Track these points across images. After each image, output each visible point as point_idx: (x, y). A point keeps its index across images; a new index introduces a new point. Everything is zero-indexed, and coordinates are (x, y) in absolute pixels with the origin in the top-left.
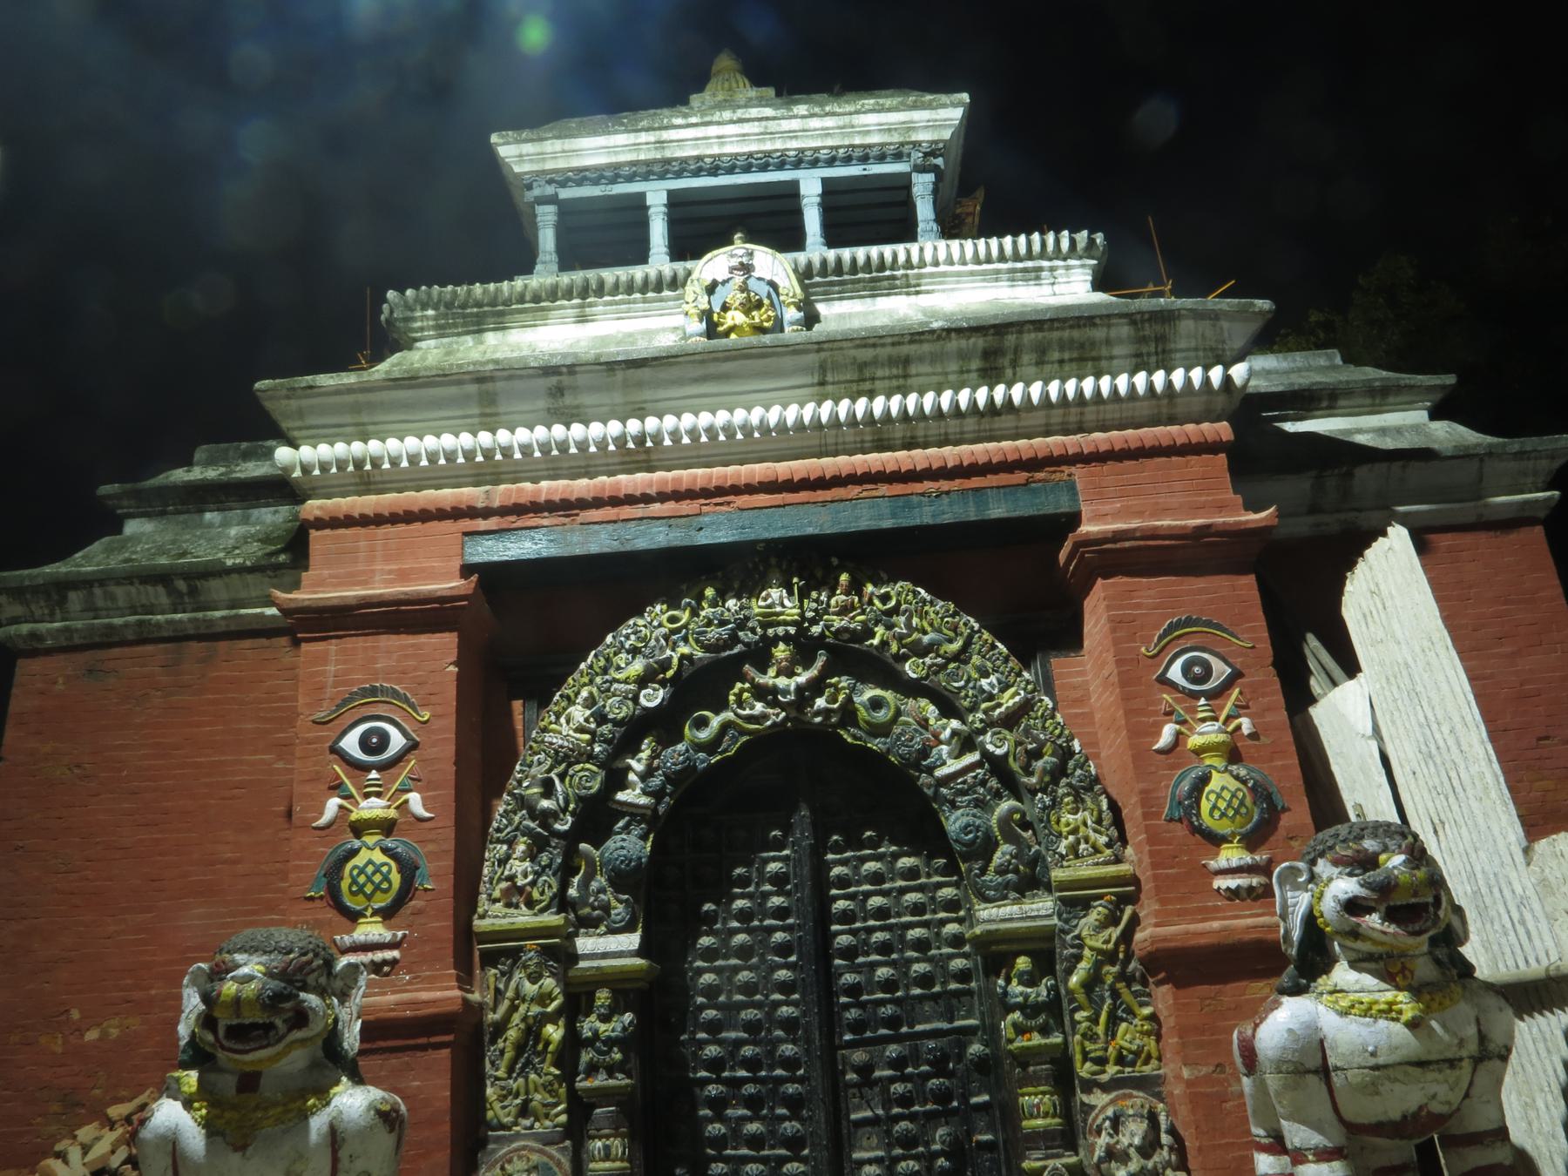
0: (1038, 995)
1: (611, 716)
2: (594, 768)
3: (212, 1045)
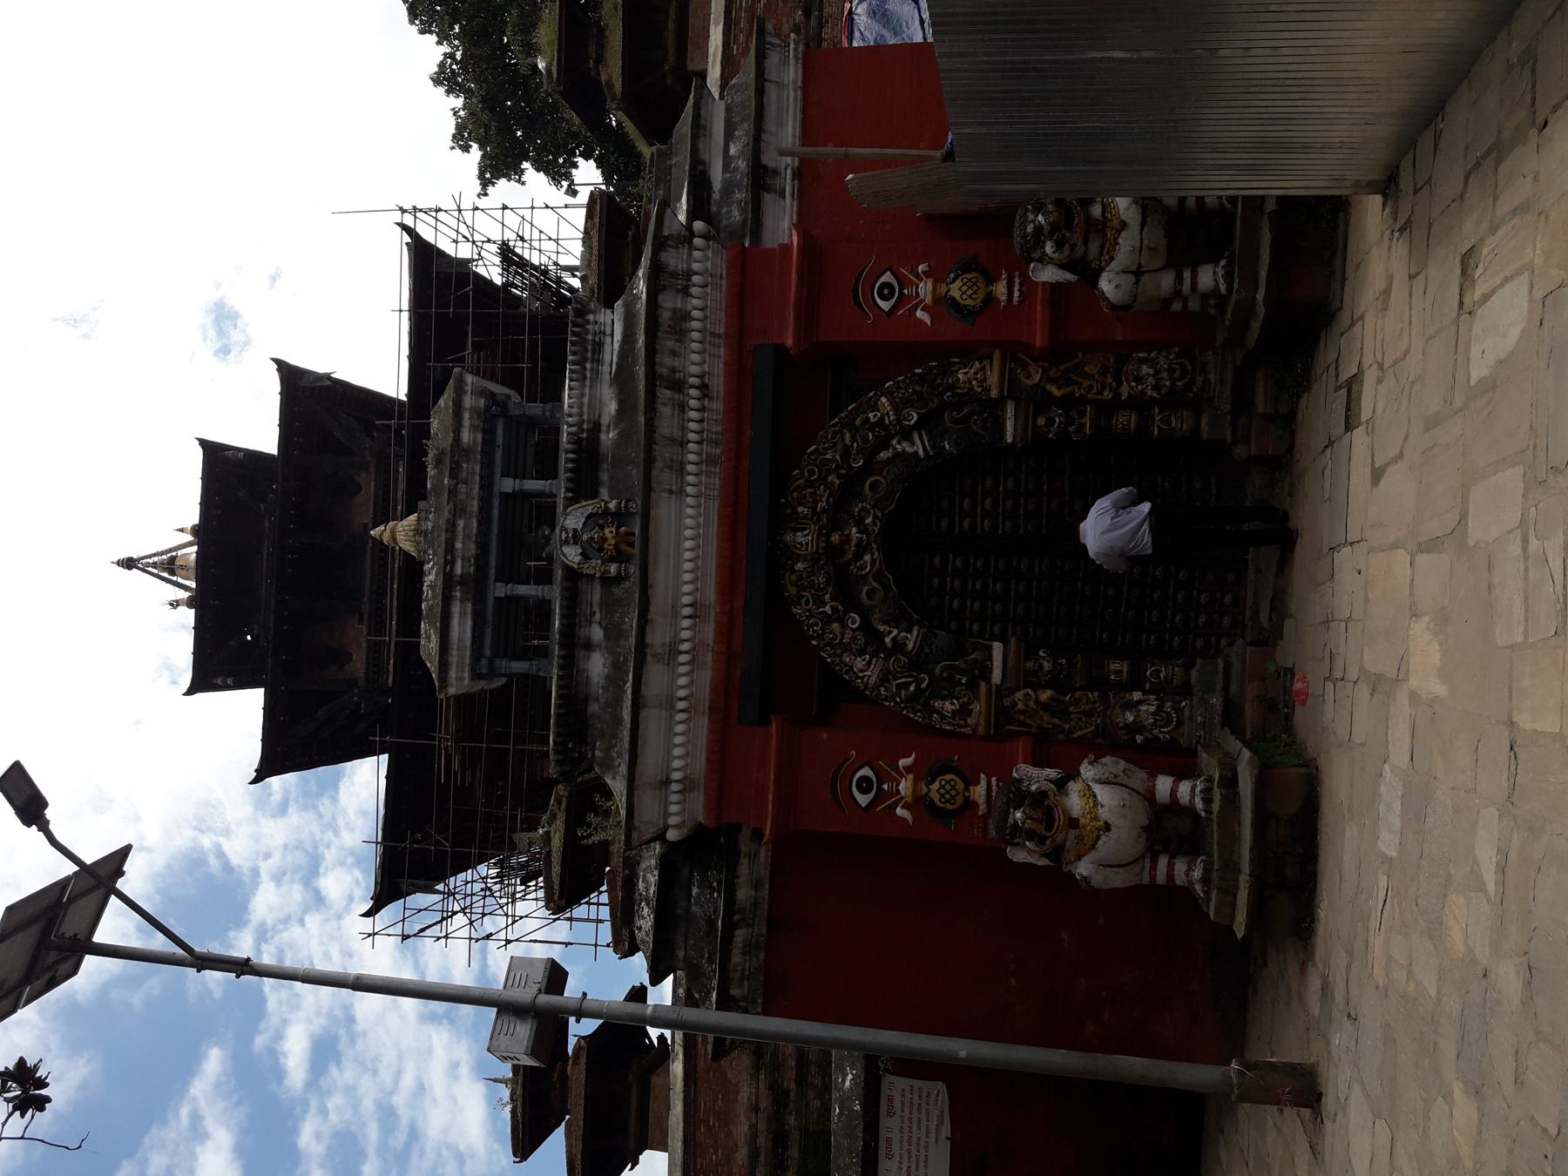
0: (1060, 415)
1: (862, 645)
2: (893, 659)
3: (1052, 842)
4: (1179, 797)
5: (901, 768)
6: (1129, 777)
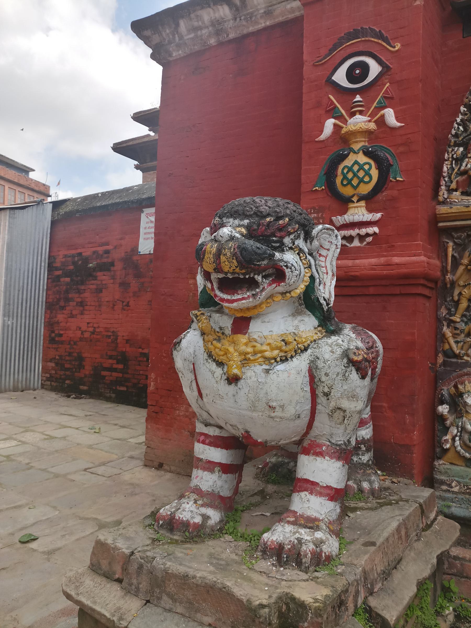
4: (303, 494)
5: (382, 112)
6: (330, 416)
